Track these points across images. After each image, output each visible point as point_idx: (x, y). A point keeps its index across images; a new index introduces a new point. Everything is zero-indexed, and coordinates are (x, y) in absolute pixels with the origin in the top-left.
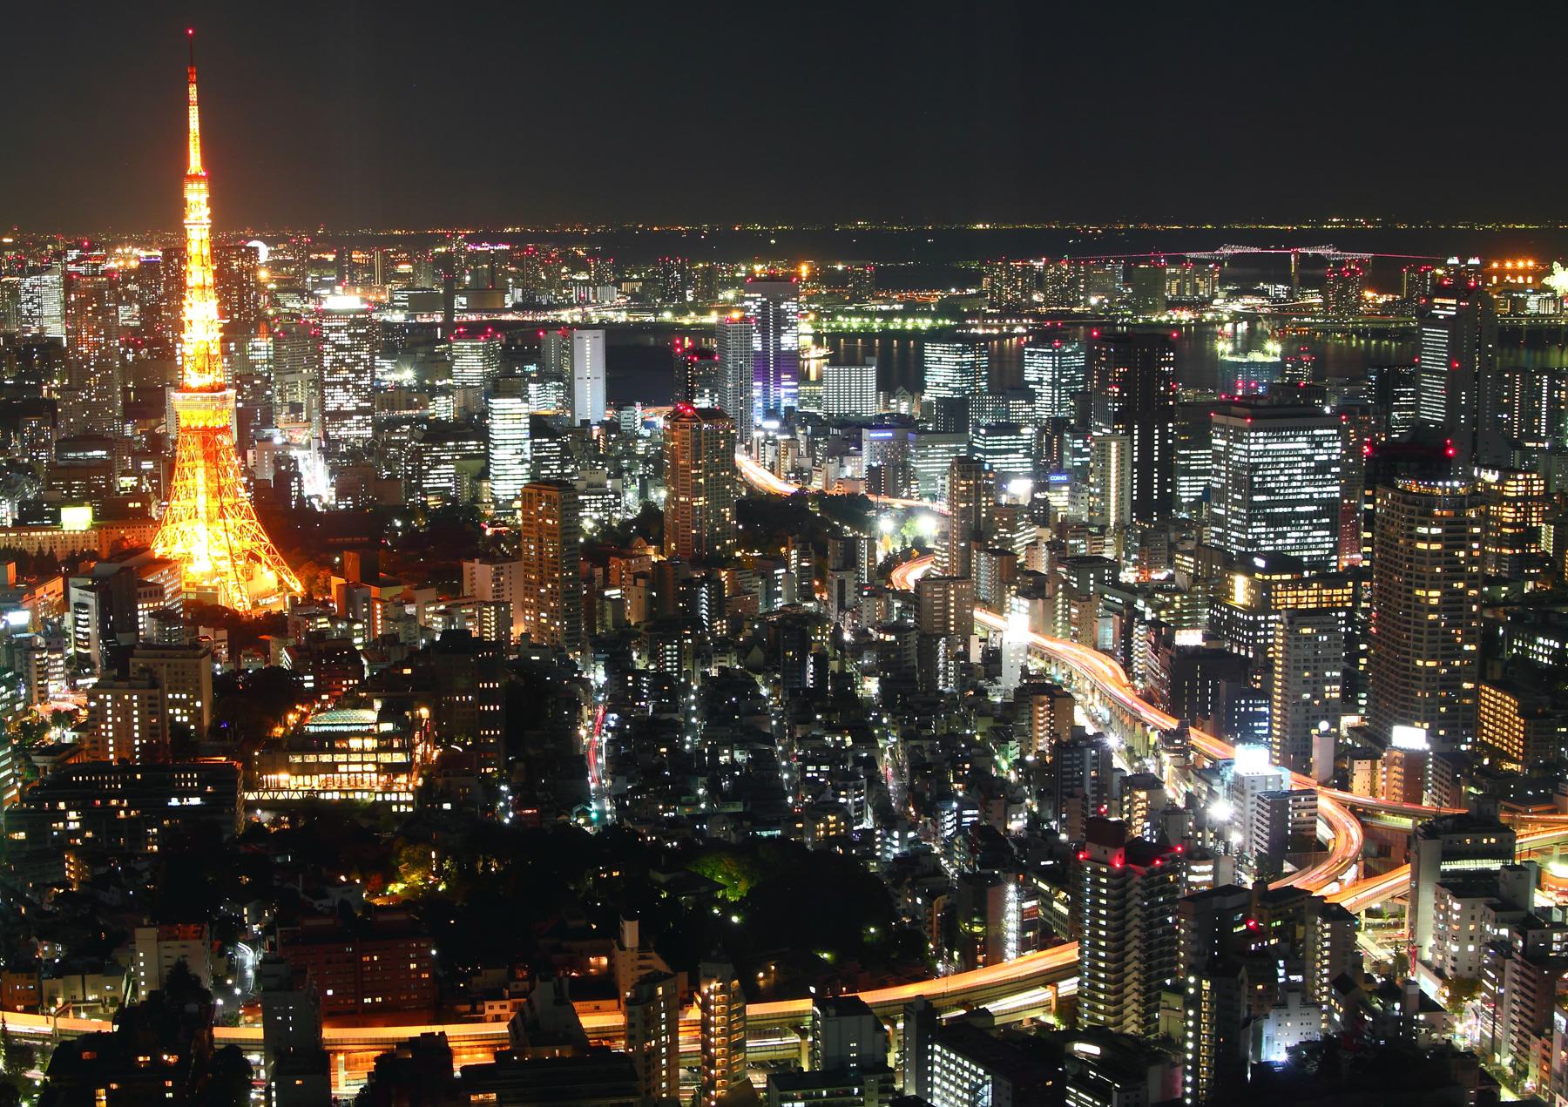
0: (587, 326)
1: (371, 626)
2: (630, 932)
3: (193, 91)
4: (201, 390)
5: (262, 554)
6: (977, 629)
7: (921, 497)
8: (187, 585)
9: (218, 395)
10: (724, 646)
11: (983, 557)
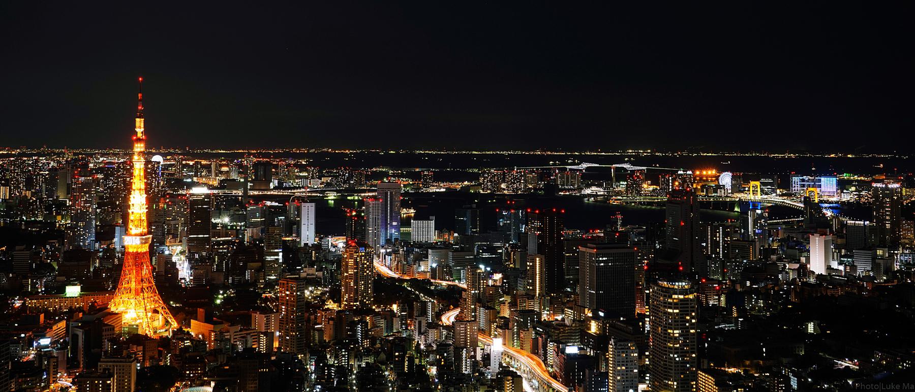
4: (136, 235)
5: (160, 309)
6: (479, 344)
10: (368, 352)
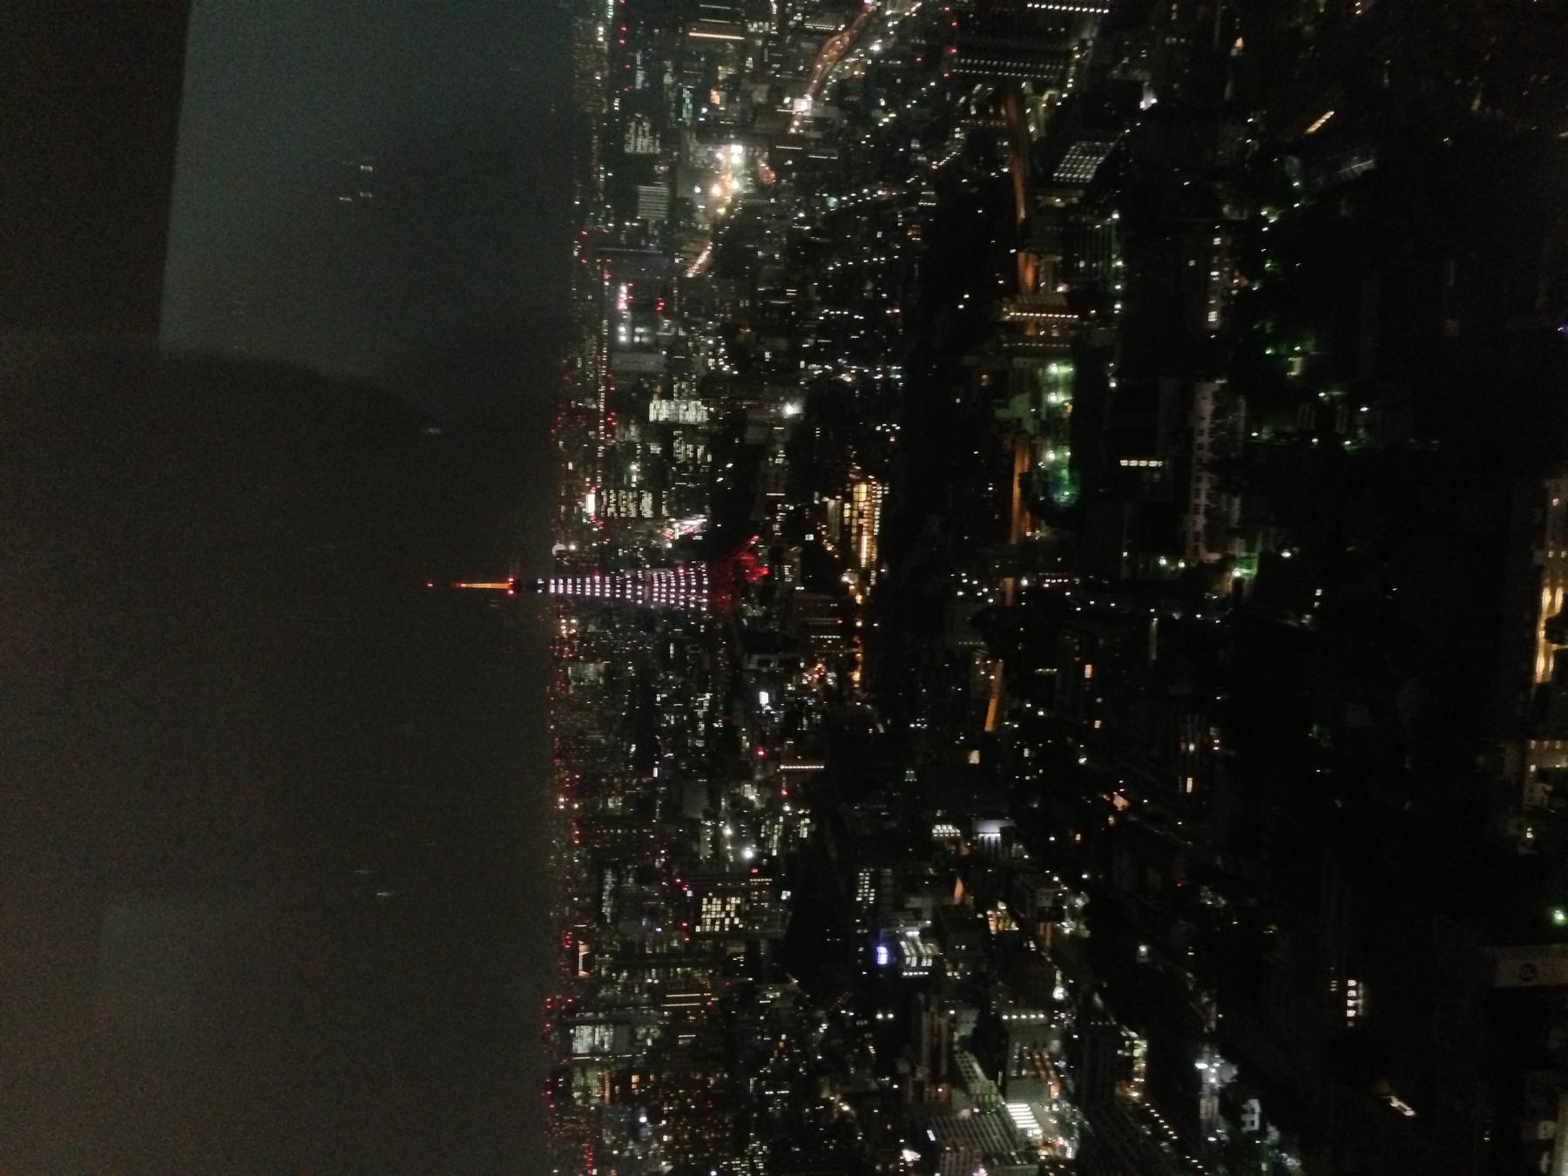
0: (609, 363)
1: (778, 500)
2: (968, 360)
11: (757, 125)
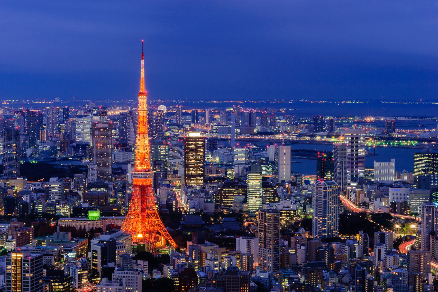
3: (143, 62)
4: (141, 171)
5: (162, 232)
7: (411, 215)
8: (134, 243)
9: (148, 173)
